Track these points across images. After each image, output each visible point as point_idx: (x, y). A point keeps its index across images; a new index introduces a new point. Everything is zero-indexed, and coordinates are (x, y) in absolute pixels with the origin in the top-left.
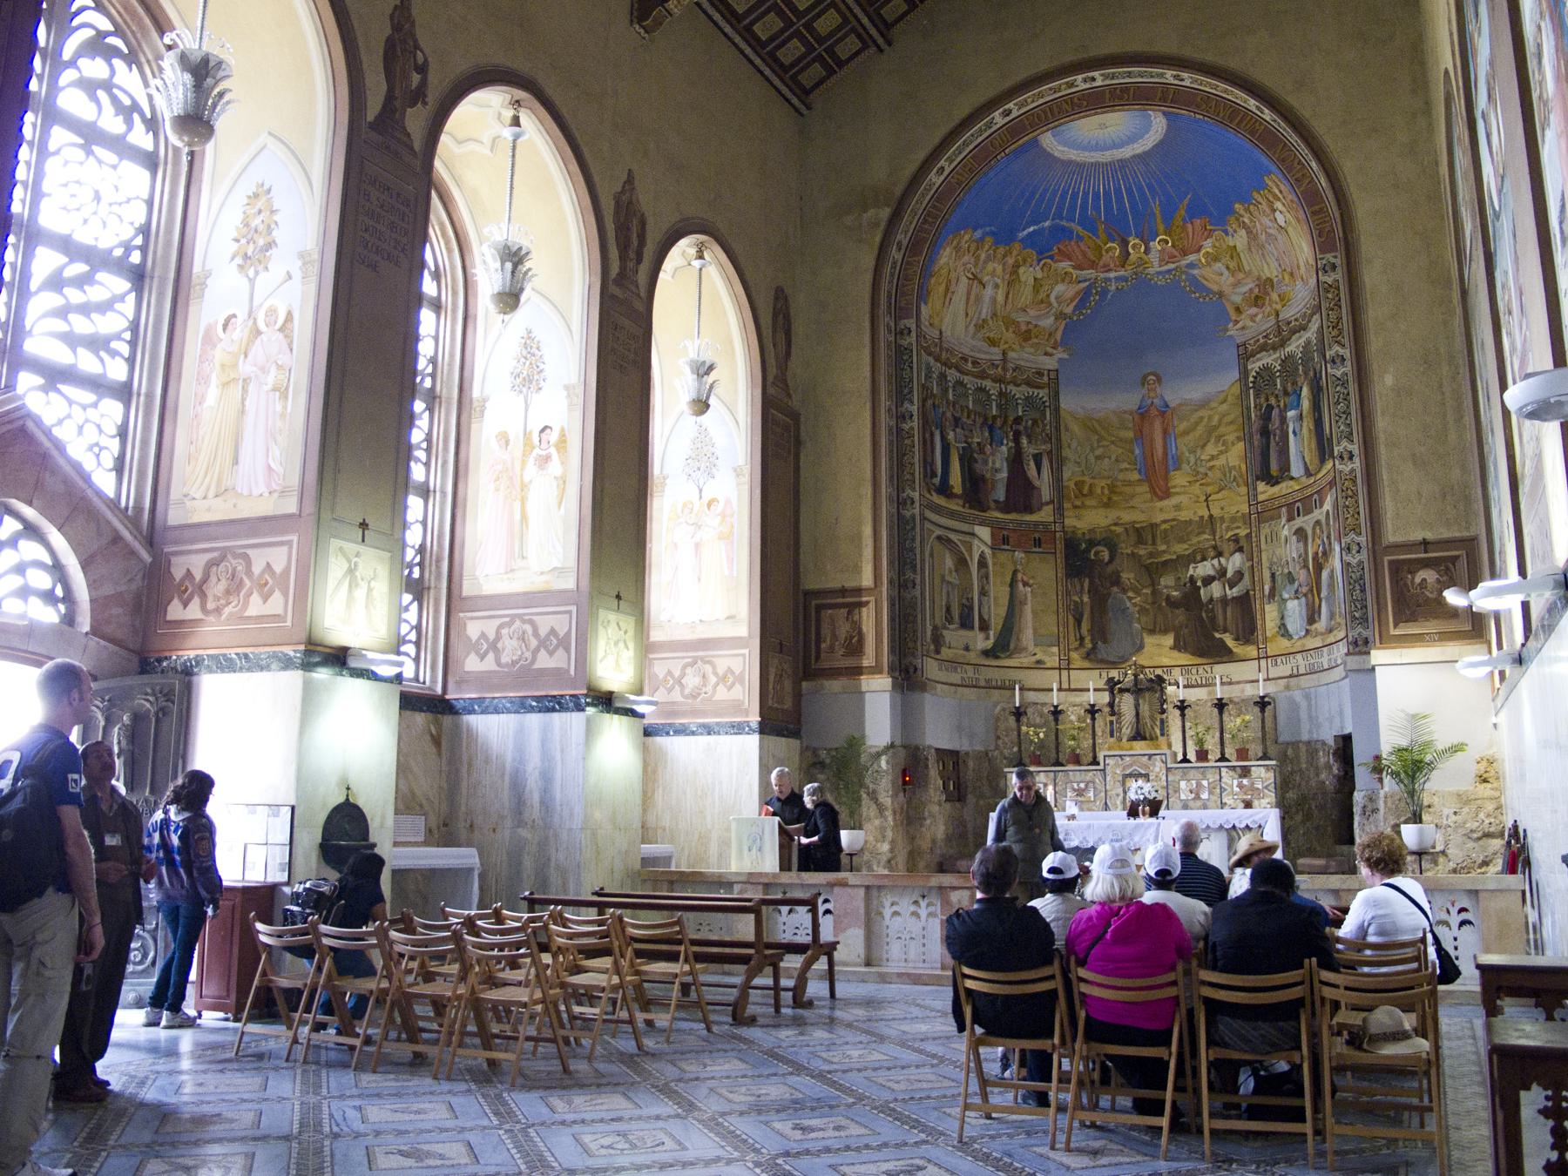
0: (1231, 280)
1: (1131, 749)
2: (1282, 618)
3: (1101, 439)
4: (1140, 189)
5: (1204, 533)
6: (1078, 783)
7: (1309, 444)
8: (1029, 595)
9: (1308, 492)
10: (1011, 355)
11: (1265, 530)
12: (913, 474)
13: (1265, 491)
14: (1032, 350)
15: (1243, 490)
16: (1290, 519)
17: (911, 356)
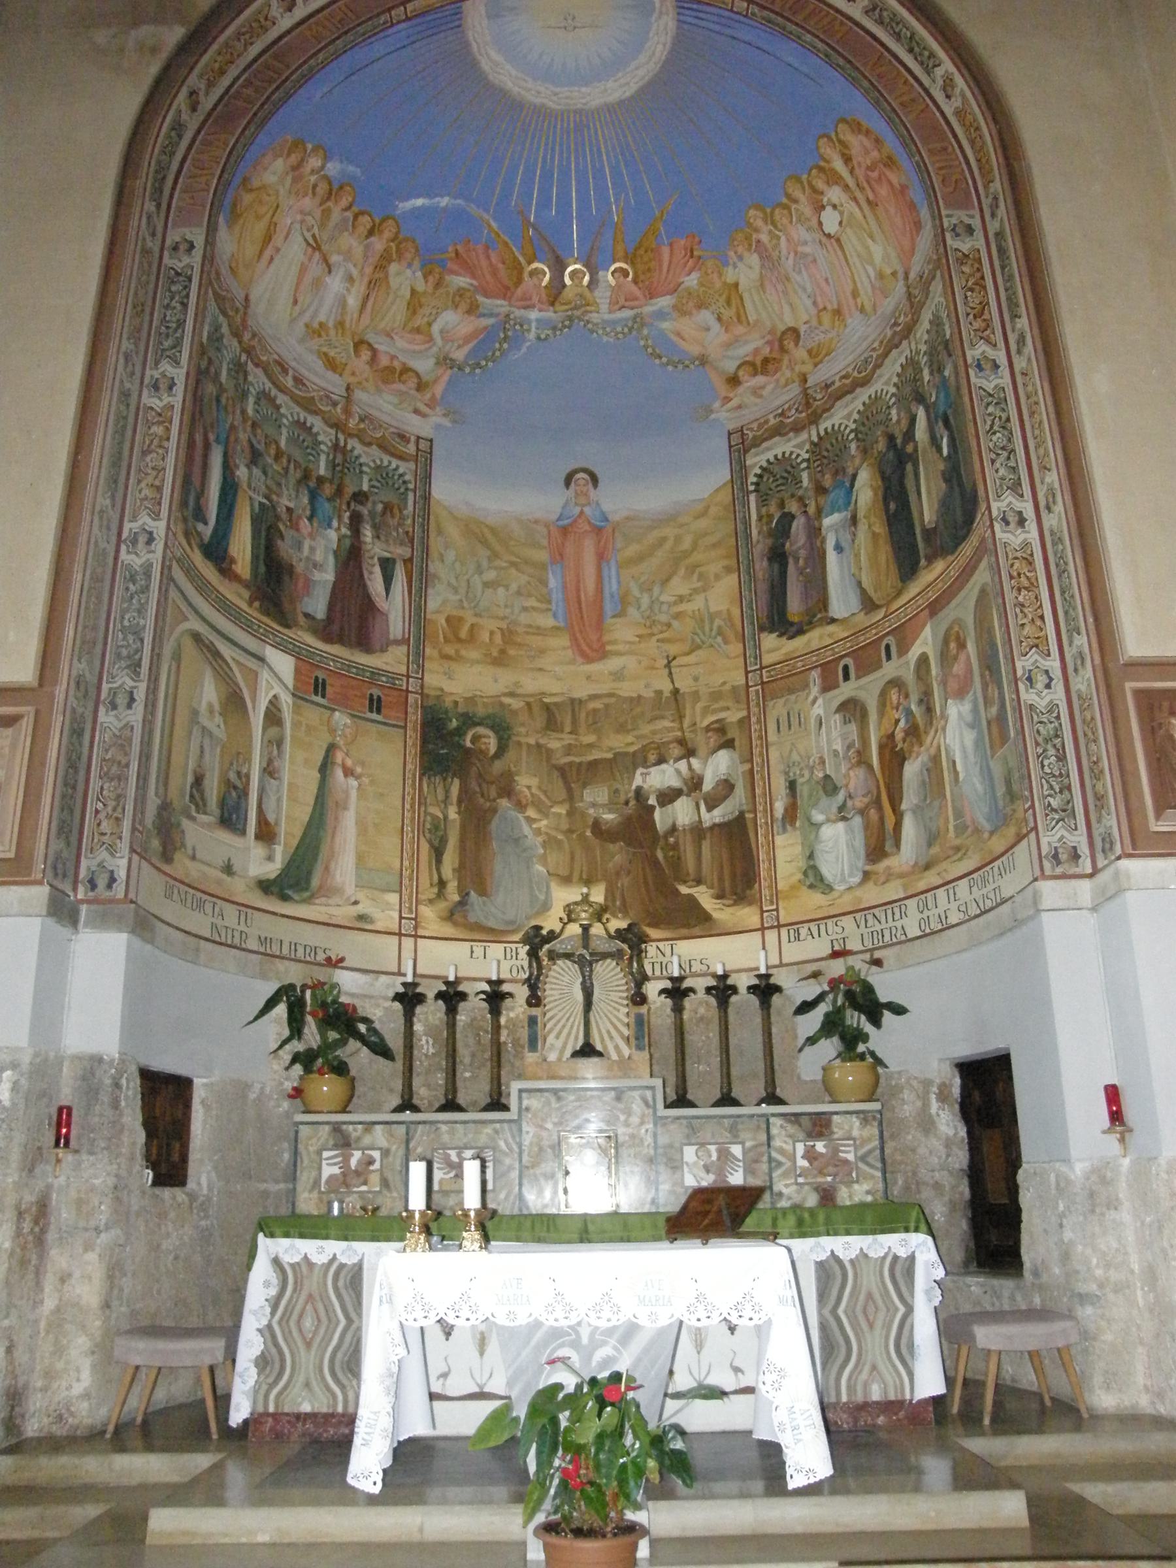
0: (724, 337)
2: (811, 856)
3: (495, 555)
5: (663, 717)
6: (460, 1149)
8: (354, 794)
9: (871, 636)
10: (359, 395)
11: (777, 709)
12: (159, 489)
13: (774, 647)
14: (396, 401)
15: (736, 648)
16: (828, 686)
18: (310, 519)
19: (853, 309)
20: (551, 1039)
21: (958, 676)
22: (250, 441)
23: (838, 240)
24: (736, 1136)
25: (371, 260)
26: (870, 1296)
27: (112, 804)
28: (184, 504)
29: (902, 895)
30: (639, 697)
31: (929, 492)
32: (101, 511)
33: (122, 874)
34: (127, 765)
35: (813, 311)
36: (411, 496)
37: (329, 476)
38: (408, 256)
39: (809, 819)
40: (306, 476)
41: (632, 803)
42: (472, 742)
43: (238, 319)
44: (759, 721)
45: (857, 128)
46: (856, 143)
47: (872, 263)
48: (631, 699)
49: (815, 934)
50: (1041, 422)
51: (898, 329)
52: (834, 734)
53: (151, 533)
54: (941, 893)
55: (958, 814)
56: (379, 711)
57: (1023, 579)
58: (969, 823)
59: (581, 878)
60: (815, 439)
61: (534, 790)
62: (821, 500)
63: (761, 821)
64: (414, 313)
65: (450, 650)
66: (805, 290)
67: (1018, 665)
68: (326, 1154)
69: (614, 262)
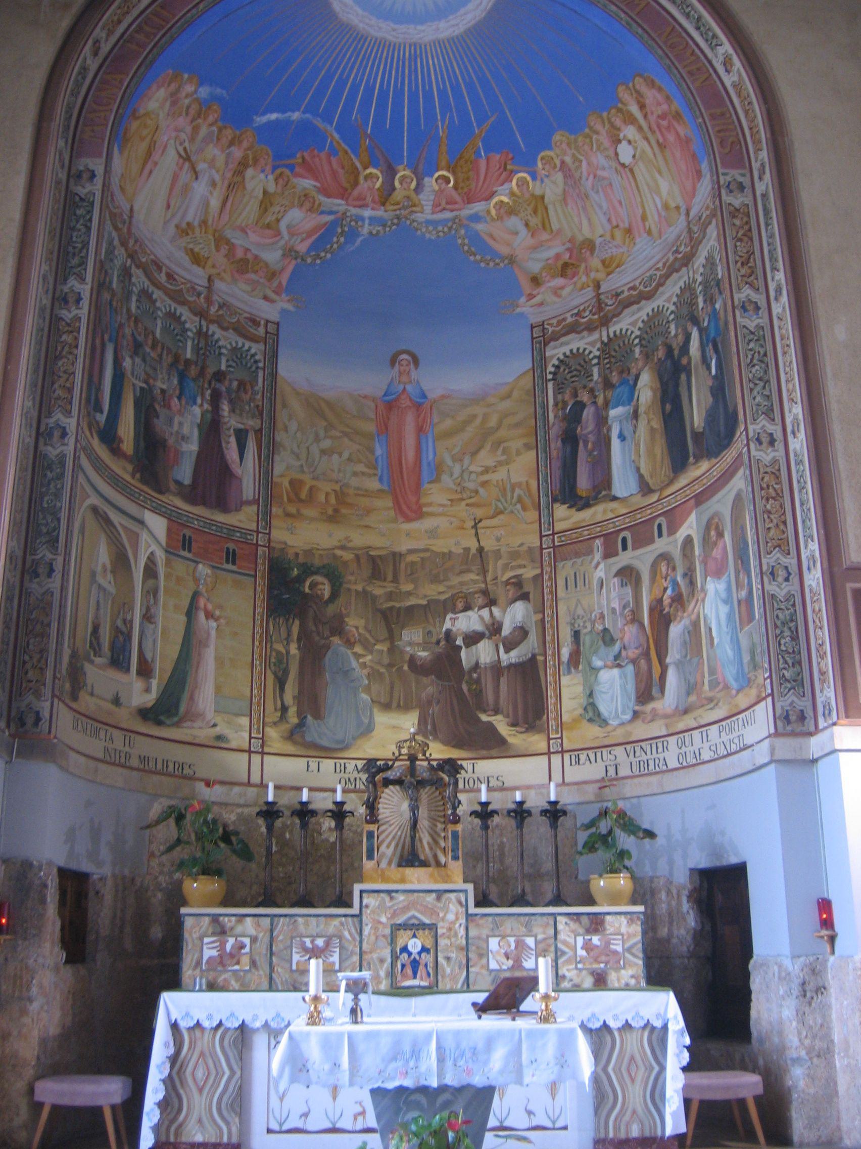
0: (530, 241)
1: (403, 880)
2: (591, 695)
3: (330, 426)
4: (428, 96)
5: (469, 571)
6: (313, 938)
7: (650, 453)
8: (213, 633)
9: (647, 514)
10: (219, 285)
11: (566, 569)
12: (70, 390)
14: (248, 288)
15: (533, 515)
16: (609, 554)
17: (90, 212)
18: (179, 398)
19: (642, 231)
20: (383, 848)
21: (716, 559)
22: (133, 334)
23: (631, 171)
24: (530, 931)
25: (231, 166)
26: (632, 1058)
27: (36, 657)
28: (88, 401)
29: (664, 732)
30: (450, 552)
31: (698, 400)
32: (27, 413)
33: (46, 714)
34: (49, 625)
35: (608, 227)
36: (261, 374)
37: (194, 358)
38: (262, 162)
39: (589, 664)
40: (177, 359)
41: (443, 643)
42: (311, 587)
43: (125, 230)
44: (550, 578)
45: (652, 84)
46: (650, 95)
47: (661, 198)
48: (444, 554)
49: (593, 759)
50: (791, 362)
51: (680, 256)
52: (613, 594)
53: (64, 428)
54: (696, 734)
55: (712, 672)
56: (234, 563)
57: (771, 490)
58: (720, 680)
59: (399, 706)
60: (605, 339)
61: (361, 631)
62: (609, 394)
63: (550, 663)
64: (266, 210)
65: (292, 510)
66: (601, 207)
67: (764, 561)
68: (206, 940)
69: (437, 171)
